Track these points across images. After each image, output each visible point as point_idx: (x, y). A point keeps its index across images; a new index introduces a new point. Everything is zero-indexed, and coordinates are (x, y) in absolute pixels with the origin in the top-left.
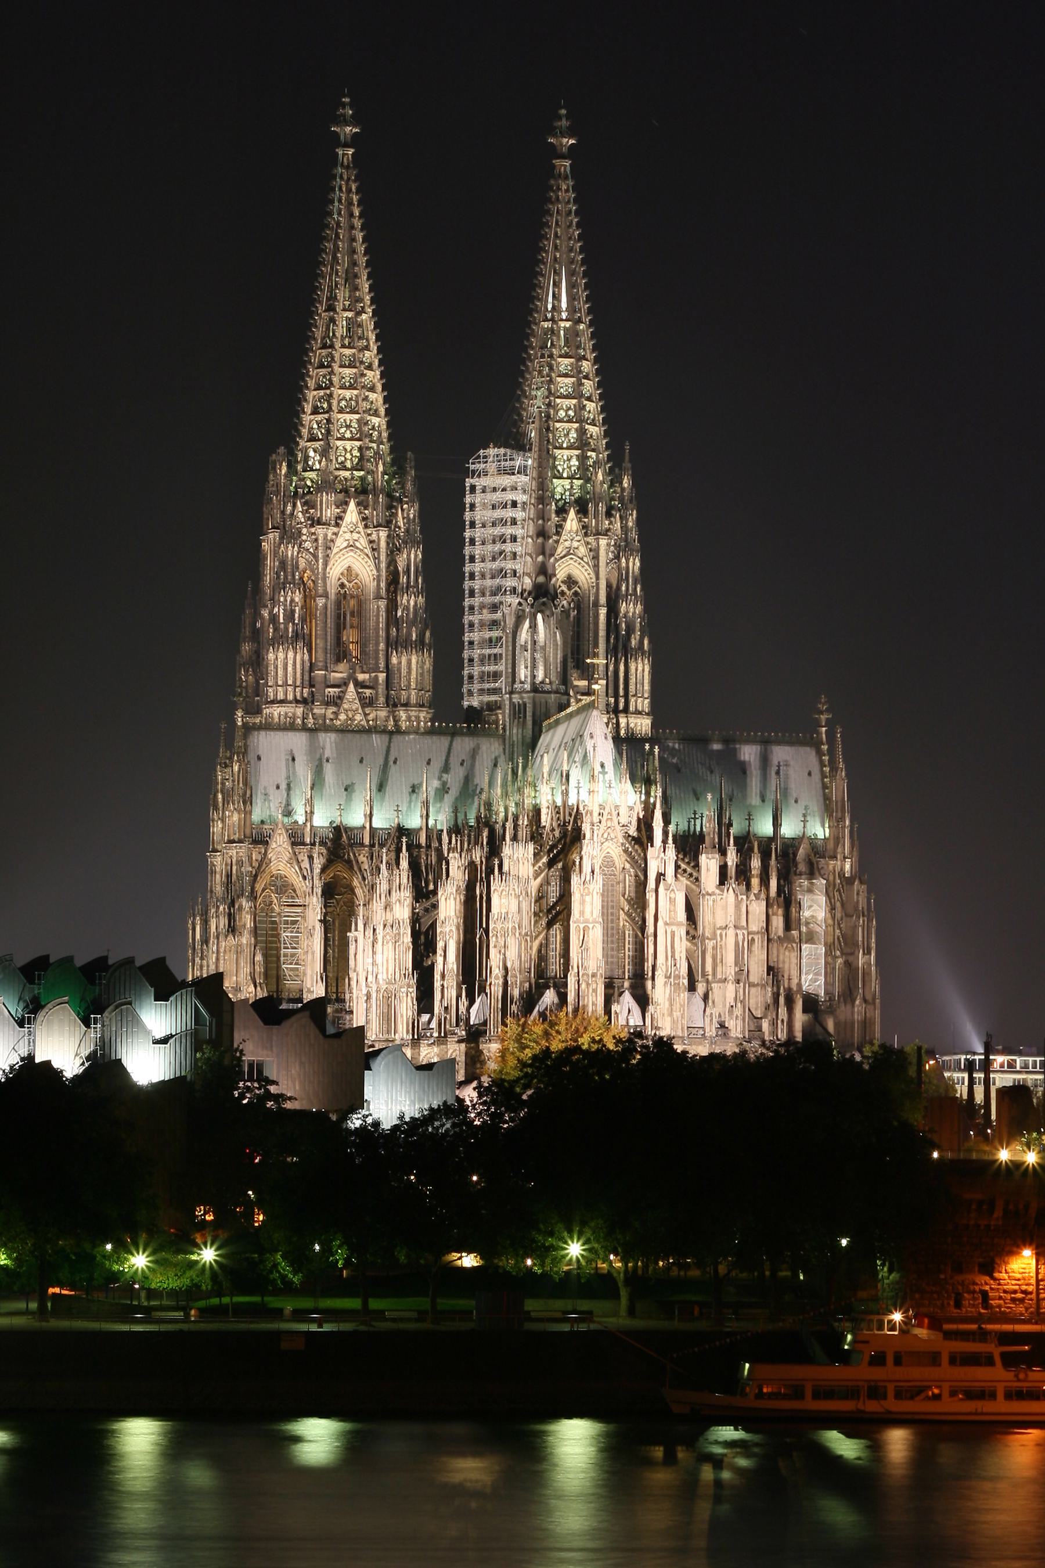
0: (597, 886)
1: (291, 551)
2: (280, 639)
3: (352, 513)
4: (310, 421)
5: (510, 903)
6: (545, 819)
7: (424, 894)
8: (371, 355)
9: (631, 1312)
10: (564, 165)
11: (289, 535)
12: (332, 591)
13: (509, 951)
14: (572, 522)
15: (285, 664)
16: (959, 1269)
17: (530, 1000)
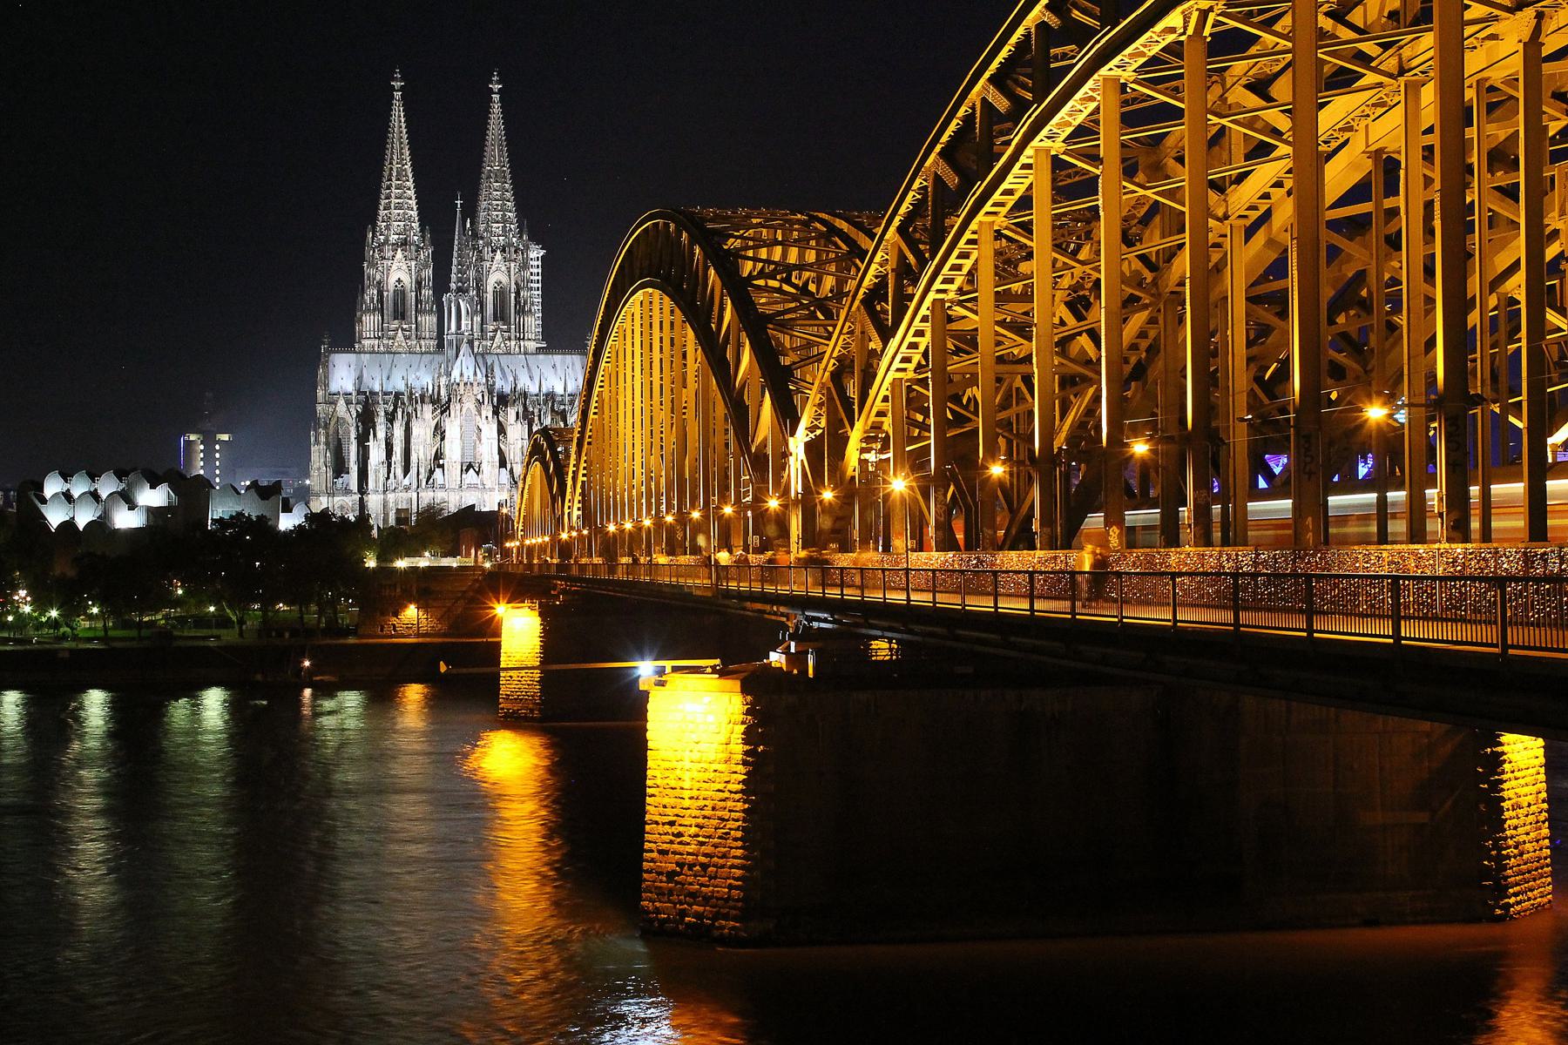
0: (457, 422)
1: (372, 271)
2: (368, 310)
3: (399, 254)
4: (382, 213)
5: (422, 431)
6: (443, 392)
7: (390, 429)
8: (410, 184)
9: (241, 634)
10: (496, 97)
11: (373, 265)
12: (391, 289)
13: (422, 450)
14: (498, 256)
15: (369, 322)
16: (383, 614)
17: (431, 472)
